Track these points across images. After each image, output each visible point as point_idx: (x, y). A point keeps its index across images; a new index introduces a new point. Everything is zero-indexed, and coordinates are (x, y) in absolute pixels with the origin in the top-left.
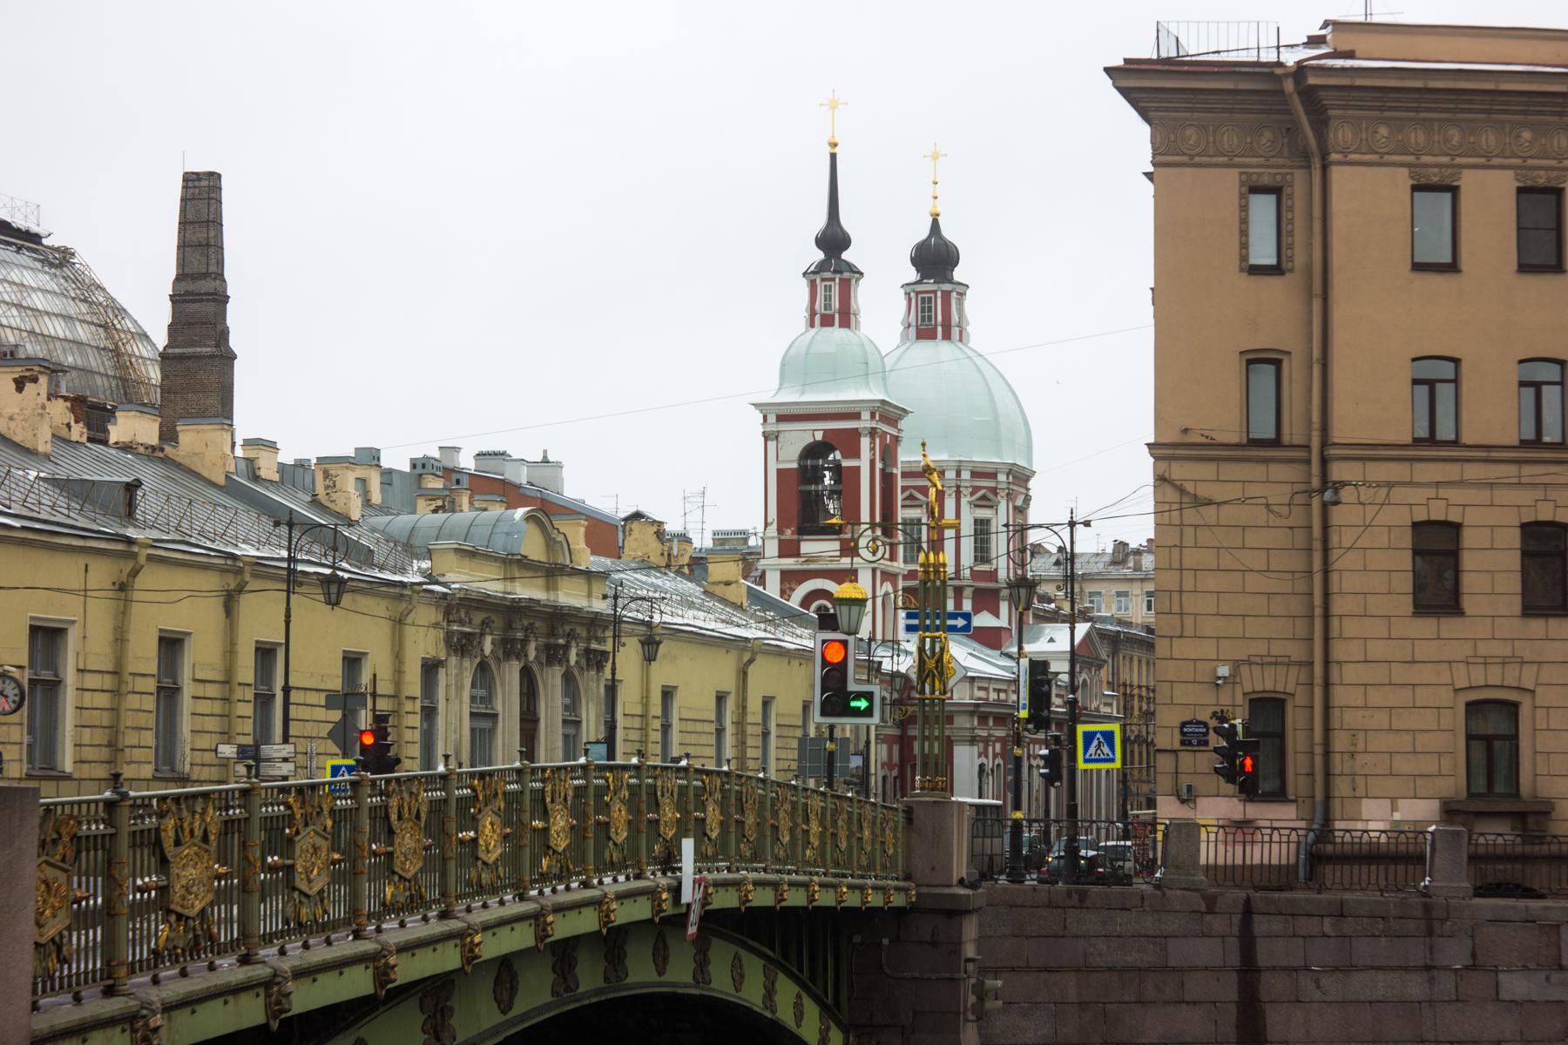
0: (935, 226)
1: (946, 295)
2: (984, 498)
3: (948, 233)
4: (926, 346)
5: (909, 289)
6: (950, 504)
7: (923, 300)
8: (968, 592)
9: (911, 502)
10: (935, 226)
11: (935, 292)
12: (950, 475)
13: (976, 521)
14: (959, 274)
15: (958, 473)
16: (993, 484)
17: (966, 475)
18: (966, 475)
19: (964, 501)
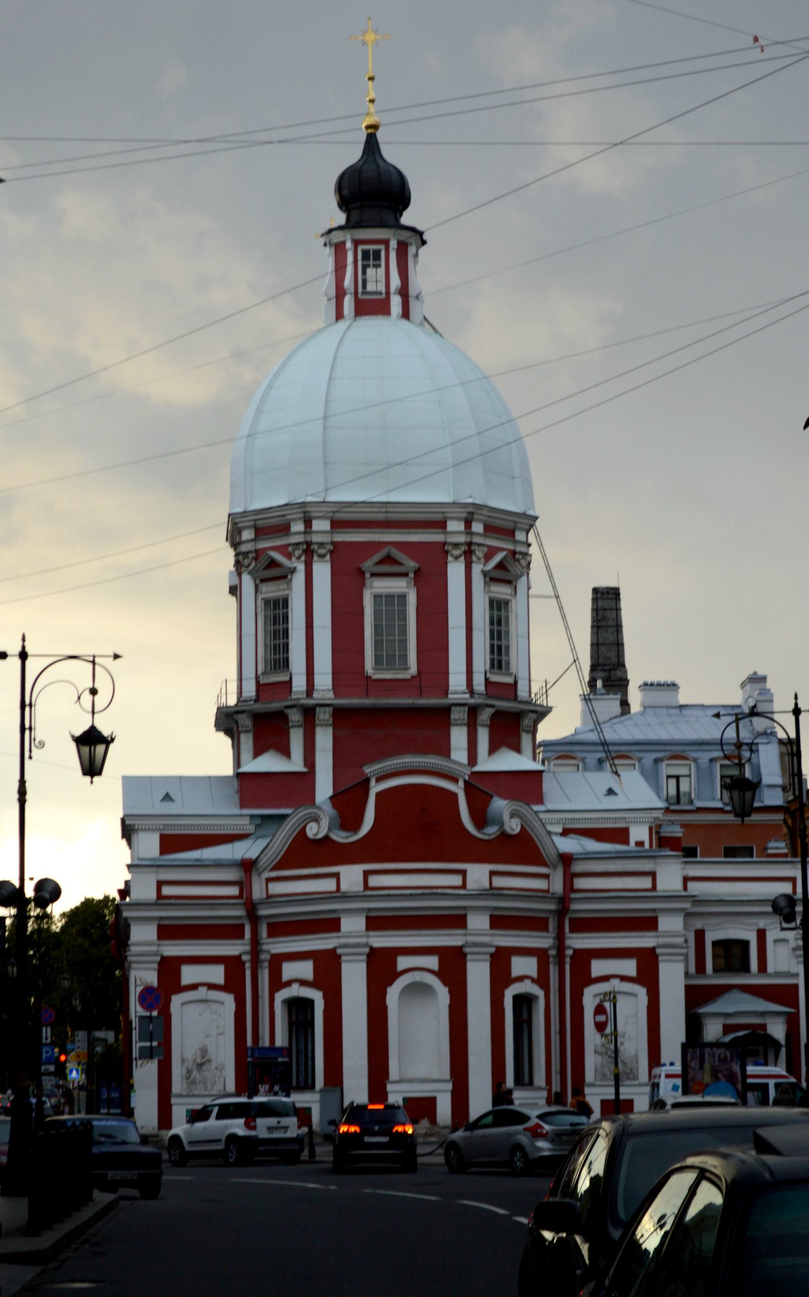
0: (372, 145)
1: (403, 248)
2: (501, 566)
3: (391, 153)
4: (370, 325)
5: (337, 237)
6: (455, 571)
7: (366, 255)
8: (485, 716)
9: (389, 565)
10: (372, 145)
11: (386, 243)
12: (455, 526)
13: (491, 602)
14: (407, 219)
15: (468, 524)
16: (510, 546)
17: (477, 527)
18: (477, 527)
19: (477, 569)
